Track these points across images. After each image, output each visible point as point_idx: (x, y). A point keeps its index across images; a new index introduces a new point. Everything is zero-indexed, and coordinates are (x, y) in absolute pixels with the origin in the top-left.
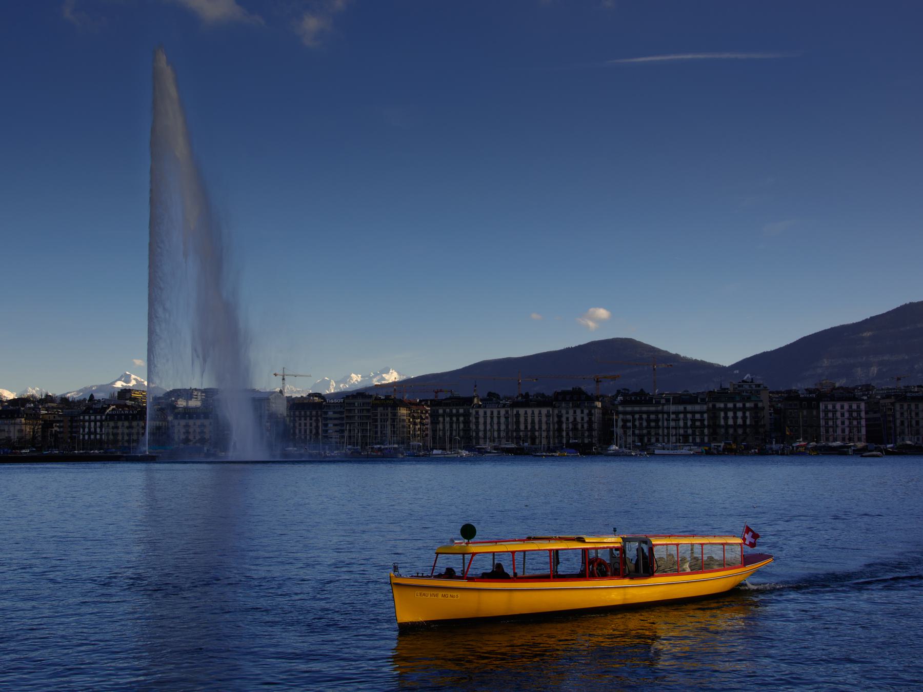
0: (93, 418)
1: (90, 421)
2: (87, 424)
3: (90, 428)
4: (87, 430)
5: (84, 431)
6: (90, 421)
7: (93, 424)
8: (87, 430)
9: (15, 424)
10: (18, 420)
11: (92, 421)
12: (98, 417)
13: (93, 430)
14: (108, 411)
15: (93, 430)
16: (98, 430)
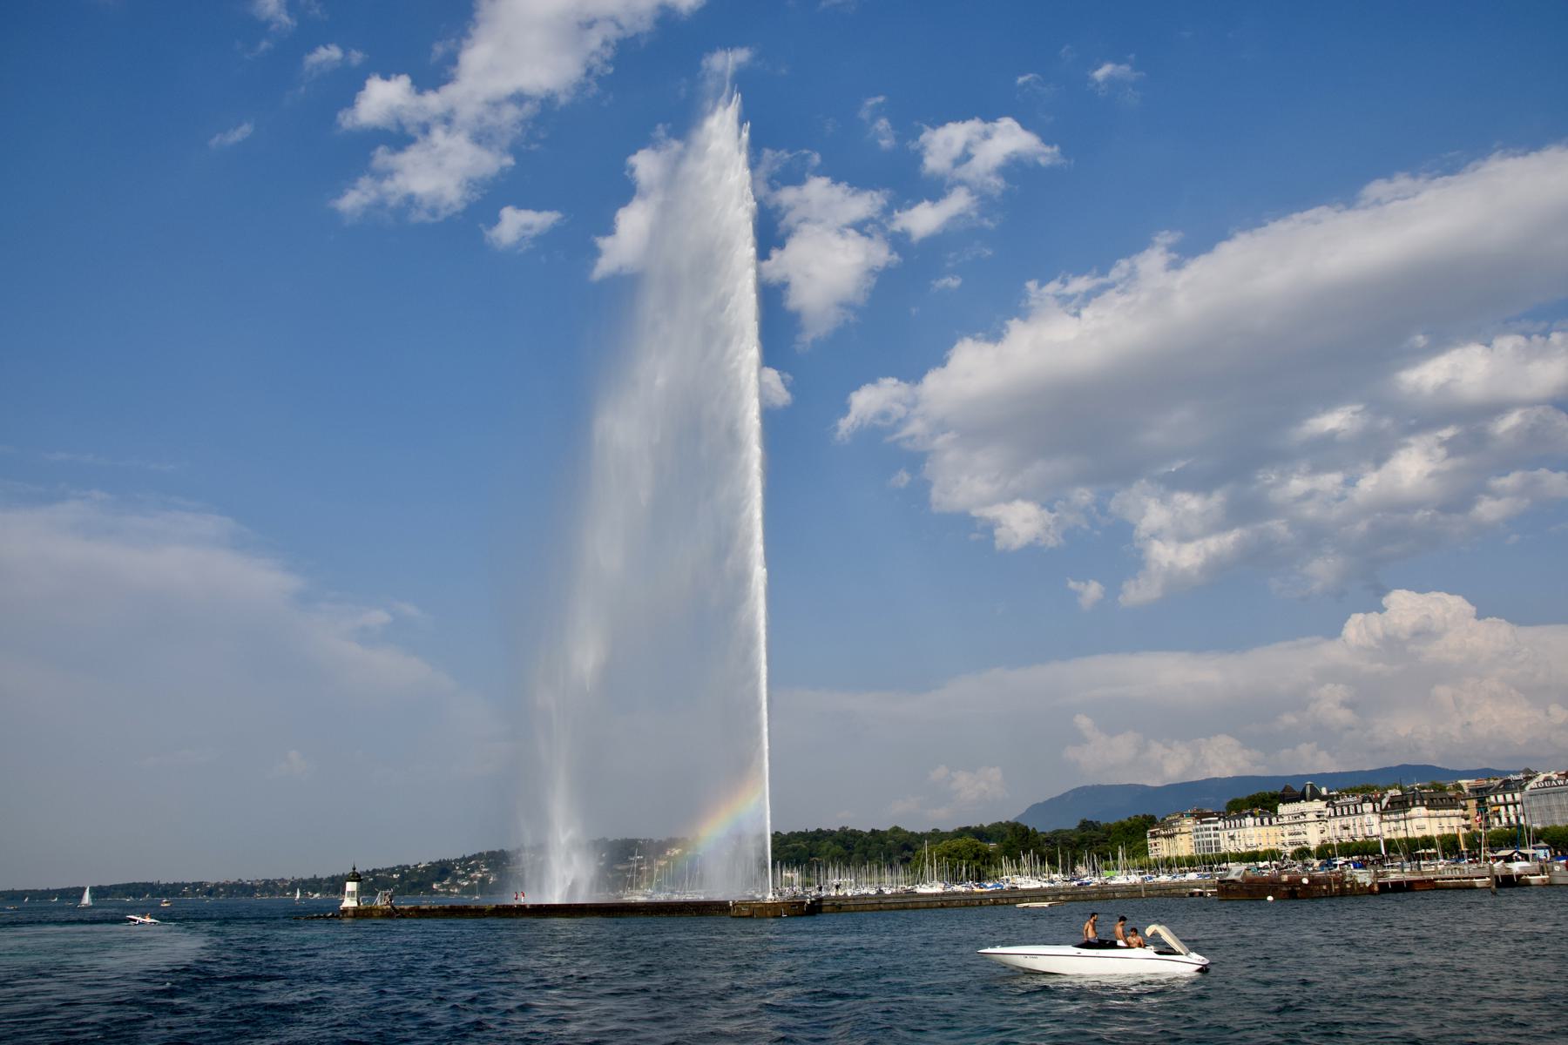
0: (1509, 797)
1: (1506, 805)
2: (1502, 809)
3: (1508, 818)
4: (1504, 820)
5: (1500, 822)
6: (1506, 805)
7: (1511, 808)
8: (1504, 820)
9: (1411, 818)
10: (1414, 811)
11: (1510, 804)
12: (1517, 796)
13: (1513, 819)
14: (1532, 784)
15: (1513, 819)
16: (1522, 821)
